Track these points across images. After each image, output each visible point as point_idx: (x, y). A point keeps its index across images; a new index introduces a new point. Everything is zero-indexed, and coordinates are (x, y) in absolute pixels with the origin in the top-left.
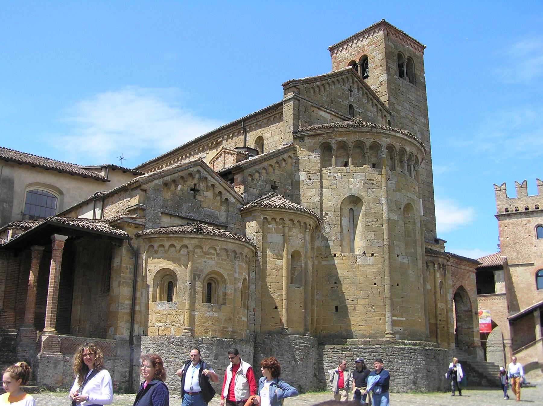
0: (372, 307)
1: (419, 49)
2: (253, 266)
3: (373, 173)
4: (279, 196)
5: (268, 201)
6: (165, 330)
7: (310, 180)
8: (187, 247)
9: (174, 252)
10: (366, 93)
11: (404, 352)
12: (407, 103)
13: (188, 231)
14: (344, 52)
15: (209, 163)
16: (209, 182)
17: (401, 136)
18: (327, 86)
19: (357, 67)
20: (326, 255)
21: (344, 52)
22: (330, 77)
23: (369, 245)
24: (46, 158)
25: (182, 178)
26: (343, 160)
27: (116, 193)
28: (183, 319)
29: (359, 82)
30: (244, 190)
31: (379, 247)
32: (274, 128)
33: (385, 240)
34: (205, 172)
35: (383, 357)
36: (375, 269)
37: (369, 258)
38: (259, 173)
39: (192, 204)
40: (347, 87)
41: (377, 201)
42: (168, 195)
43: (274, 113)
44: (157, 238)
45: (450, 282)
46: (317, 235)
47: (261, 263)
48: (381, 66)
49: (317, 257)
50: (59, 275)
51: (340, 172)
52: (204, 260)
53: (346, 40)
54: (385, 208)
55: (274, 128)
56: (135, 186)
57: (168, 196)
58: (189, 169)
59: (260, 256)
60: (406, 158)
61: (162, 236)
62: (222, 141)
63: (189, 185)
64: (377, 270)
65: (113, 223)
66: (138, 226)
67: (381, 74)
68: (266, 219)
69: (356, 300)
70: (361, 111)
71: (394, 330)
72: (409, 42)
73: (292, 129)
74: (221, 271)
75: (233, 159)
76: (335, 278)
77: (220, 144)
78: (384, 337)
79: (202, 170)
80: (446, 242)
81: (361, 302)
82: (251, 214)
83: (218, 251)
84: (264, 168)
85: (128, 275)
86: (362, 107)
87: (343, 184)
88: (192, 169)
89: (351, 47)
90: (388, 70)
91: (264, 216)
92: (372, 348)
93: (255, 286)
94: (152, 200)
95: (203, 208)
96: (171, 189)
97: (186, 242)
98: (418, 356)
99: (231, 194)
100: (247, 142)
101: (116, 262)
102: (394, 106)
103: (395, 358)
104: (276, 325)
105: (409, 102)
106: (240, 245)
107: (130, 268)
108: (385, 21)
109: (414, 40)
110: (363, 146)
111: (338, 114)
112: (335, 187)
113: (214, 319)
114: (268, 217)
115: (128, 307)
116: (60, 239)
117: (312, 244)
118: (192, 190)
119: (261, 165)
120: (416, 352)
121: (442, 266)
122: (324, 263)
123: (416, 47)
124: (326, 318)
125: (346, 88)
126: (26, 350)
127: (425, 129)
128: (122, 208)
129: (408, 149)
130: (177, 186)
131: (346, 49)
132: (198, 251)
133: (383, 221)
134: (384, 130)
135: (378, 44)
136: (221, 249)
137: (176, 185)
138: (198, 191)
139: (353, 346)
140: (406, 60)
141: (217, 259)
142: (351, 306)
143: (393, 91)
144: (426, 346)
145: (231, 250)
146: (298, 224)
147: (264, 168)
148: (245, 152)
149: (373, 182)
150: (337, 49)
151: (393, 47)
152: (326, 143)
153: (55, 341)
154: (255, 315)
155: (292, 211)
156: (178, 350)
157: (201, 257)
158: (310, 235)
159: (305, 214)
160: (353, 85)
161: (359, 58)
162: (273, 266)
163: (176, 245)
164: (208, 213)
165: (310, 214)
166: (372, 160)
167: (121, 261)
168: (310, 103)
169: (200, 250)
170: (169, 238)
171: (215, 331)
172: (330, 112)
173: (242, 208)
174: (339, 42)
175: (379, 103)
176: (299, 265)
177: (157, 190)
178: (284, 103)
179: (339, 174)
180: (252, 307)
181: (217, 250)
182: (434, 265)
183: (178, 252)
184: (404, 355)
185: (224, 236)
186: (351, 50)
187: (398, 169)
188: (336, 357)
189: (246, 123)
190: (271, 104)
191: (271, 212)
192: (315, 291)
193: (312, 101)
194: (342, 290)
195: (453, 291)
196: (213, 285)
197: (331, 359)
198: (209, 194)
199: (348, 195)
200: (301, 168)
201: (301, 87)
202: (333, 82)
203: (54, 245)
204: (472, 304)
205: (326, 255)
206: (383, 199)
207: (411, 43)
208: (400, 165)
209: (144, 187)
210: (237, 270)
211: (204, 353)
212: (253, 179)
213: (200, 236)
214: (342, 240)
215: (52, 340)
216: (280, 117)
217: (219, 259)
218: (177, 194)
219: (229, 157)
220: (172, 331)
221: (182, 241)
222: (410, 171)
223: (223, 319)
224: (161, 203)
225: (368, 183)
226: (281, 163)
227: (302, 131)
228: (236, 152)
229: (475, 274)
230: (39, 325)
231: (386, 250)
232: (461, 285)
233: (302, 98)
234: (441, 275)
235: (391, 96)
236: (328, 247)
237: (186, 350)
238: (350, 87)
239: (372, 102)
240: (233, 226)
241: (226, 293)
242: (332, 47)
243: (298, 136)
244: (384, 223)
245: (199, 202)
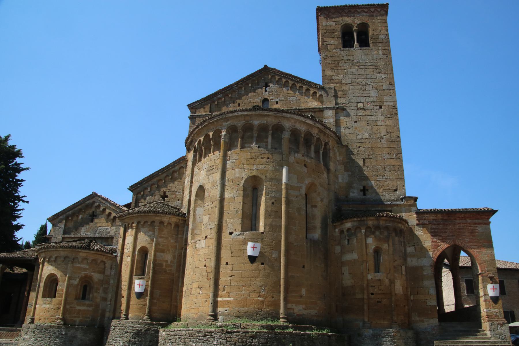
25: (81, 210)
31: (211, 228)
37: (202, 241)
64: (207, 252)
72: (359, 10)
88: (88, 202)
130: (78, 217)
144: (248, 327)
149: (213, 168)
155: (137, 215)
159: (149, 214)
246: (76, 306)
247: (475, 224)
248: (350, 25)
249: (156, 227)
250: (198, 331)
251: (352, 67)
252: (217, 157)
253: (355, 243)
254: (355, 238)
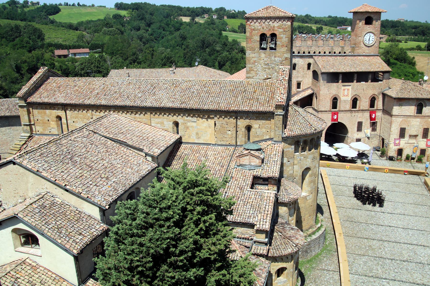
7: (289, 161)
21: (257, 24)
41: (315, 167)
89: (264, 23)
112: (300, 164)
179: (302, 157)
186: (264, 25)
199: (306, 167)
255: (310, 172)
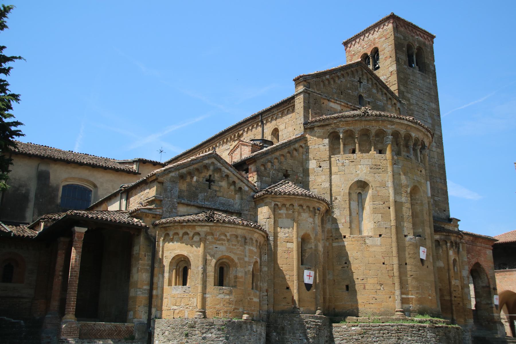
0: (381, 286)
1: (429, 39)
2: (265, 249)
3: (379, 158)
4: (290, 184)
5: (279, 189)
6: (180, 313)
7: (320, 167)
8: (198, 234)
9: (188, 239)
10: (376, 84)
11: (413, 329)
12: (416, 91)
13: (200, 220)
14: (357, 46)
15: (228, 155)
16: (223, 173)
17: (406, 122)
18: (337, 79)
19: (369, 59)
20: (336, 237)
21: (357, 45)
22: (339, 70)
23: (377, 227)
24: (86, 154)
25: (197, 170)
26: (351, 147)
27: (139, 186)
28: (197, 301)
29: (368, 74)
30: (257, 179)
31: (386, 228)
32: (287, 120)
33: (392, 222)
34: (219, 164)
35: (392, 335)
36: (384, 249)
37: (376, 238)
38: (271, 162)
39: (207, 194)
40: (357, 79)
42: (184, 186)
43: (288, 106)
44: (171, 227)
45: (466, 259)
46: (327, 218)
47: (273, 247)
48: (390, 57)
49: (328, 239)
50: (79, 265)
51: (347, 158)
52: (215, 246)
53: (359, 34)
54: (391, 191)
55: (287, 120)
56: (152, 179)
57: (184, 187)
58: (204, 162)
59: (271, 240)
60: (411, 144)
61: (176, 224)
62: (242, 134)
63: (204, 176)
64: (385, 250)
65: (133, 214)
66: (156, 216)
67: (390, 65)
68: (277, 205)
69: (365, 279)
70: (370, 101)
71: (404, 307)
72: (418, 33)
73: (302, 121)
74: (232, 256)
75: (248, 150)
76: (345, 258)
77: (241, 137)
78: (393, 314)
79: (216, 162)
80: (459, 221)
81: (371, 281)
82: (263, 201)
83: (229, 237)
84: (276, 158)
85: (146, 262)
86: (371, 97)
87: (351, 170)
90: (398, 60)
91: (275, 203)
92: (381, 326)
93: (267, 268)
94: (169, 192)
95: (218, 197)
96: (187, 181)
97: (198, 229)
98: (427, 334)
99: (244, 183)
100: (264, 133)
101: (136, 250)
102: (404, 94)
103: (404, 335)
104: (289, 304)
105: (419, 90)
106: (248, 231)
107: (148, 255)
108: (394, 14)
109: (423, 30)
110: (369, 134)
111: (348, 104)
112: (343, 173)
113: (225, 301)
114: (279, 204)
115: (146, 292)
116: (80, 230)
117: (323, 227)
118: (207, 181)
119: (273, 155)
120: (425, 329)
121: (454, 245)
122: (335, 244)
123: (426, 37)
124: (338, 297)
125: (355, 80)
126: (50, 337)
127: (435, 114)
128: (143, 199)
129: (413, 135)
130: (192, 178)
131: (358, 43)
132: (209, 237)
133: (389, 203)
134: (389, 118)
135: (388, 36)
136: (231, 235)
137: (192, 176)
138: (214, 181)
139: (363, 324)
140: (415, 50)
141: (227, 244)
142: (361, 284)
143: (402, 79)
144: (437, 323)
145: (241, 235)
146: (307, 210)
147: (276, 158)
148: (260, 143)
149: (379, 167)
150: (350, 43)
151: (402, 38)
152: (334, 132)
153: (73, 328)
154: (268, 295)
155: (301, 197)
156: (191, 332)
157: (212, 243)
158: (320, 219)
159: (314, 200)
160: (362, 76)
161: (371, 51)
162: (284, 249)
163: (189, 233)
164: (222, 201)
165: (319, 199)
166: (379, 146)
167: (140, 249)
168: (320, 96)
169: (212, 237)
170: (183, 227)
171: (226, 312)
172: (339, 102)
173: (255, 196)
174: (352, 37)
175: (389, 93)
176: (309, 247)
177: (173, 181)
178: (295, 97)
179: (347, 161)
180: (265, 288)
181: (227, 236)
182: (446, 243)
183: (191, 239)
184: (413, 332)
185: (234, 223)
187: (404, 153)
188: (347, 335)
189: (263, 117)
190: (285, 98)
191: (281, 198)
192: (327, 271)
193: (322, 94)
194: (351, 270)
195: (469, 268)
196: (225, 269)
197: (342, 336)
198: (224, 184)
199: (356, 180)
200: (311, 156)
201: (312, 81)
202: (343, 75)
203: (75, 237)
204: (490, 280)
205: (336, 237)
206: (389, 182)
207: (421, 33)
208: (406, 150)
209: (161, 179)
210: (247, 254)
211: (215, 334)
212: (265, 169)
213: (211, 224)
214: (351, 222)
215: (71, 326)
216: (293, 110)
217: (229, 245)
218: (193, 185)
219: (245, 149)
220: (186, 314)
221: (195, 229)
222: (416, 155)
223: (234, 301)
224: (177, 194)
225: (374, 168)
226: (293, 152)
227: (312, 122)
228: (250, 144)
229: (491, 251)
230: (62, 312)
231: (394, 230)
232: (477, 261)
233: (311, 91)
234: (454, 253)
235: (400, 85)
236: (338, 229)
237: (198, 331)
238: (360, 78)
239: (382, 92)
240: (246, 212)
241: (236, 276)
242: (346, 42)
243: (309, 127)
244: (391, 205)
245: (214, 192)
246: (253, 297)
247: (486, 248)
248: (412, 45)
249: (316, 215)
250: (411, 326)
251: (416, 89)
252: (382, 157)
253: (441, 253)
254: (441, 249)
255: (370, 192)
